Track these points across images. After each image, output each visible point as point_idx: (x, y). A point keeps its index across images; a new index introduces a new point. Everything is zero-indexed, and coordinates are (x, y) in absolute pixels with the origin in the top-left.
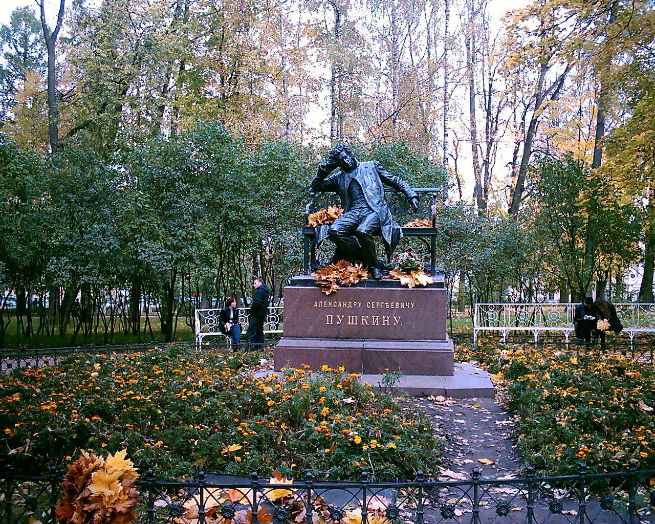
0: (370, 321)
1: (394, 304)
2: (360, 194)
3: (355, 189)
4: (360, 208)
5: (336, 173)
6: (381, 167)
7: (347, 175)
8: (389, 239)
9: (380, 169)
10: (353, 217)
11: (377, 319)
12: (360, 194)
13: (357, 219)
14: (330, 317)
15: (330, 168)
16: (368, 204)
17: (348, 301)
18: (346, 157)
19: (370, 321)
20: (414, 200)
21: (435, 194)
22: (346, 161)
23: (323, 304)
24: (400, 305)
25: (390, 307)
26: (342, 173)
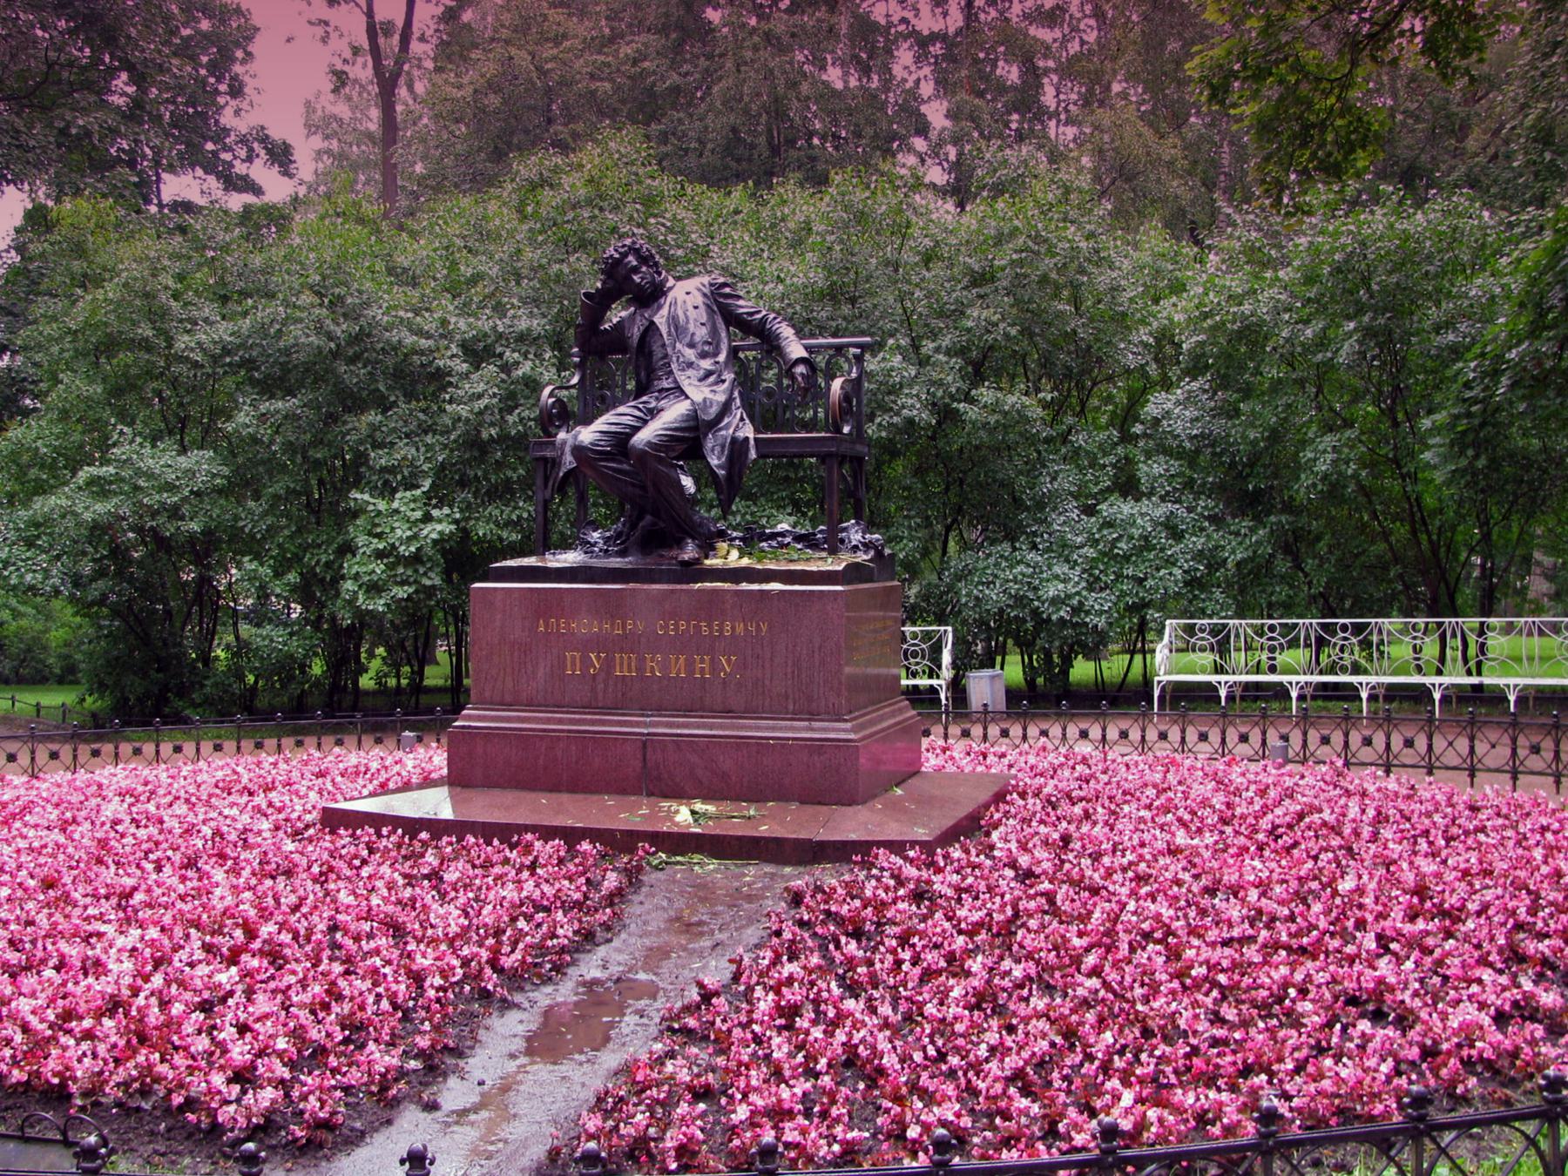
0: (665, 667)
1: (721, 626)
11: (682, 658)
14: (573, 658)
16: (675, 381)
18: (635, 270)
19: (665, 667)
22: (637, 278)
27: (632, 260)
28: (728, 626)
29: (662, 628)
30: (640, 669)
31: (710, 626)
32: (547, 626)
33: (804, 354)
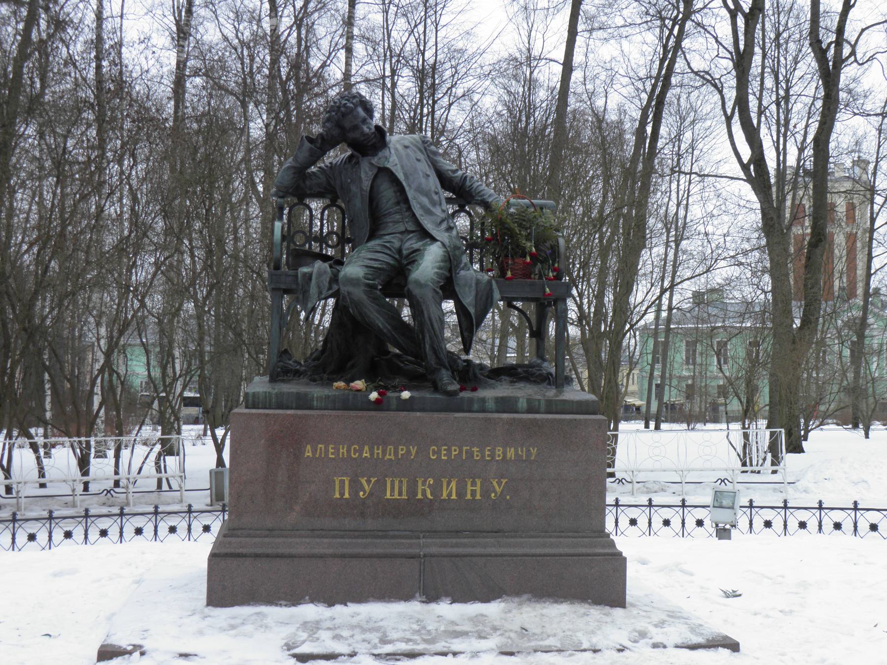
0: (436, 489)
2: (398, 203)
3: (387, 193)
4: (402, 233)
7: (366, 159)
8: (468, 300)
10: (389, 252)
13: (397, 256)
15: (322, 144)
17: (385, 444)
19: (436, 489)
23: (327, 451)
24: (505, 453)
25: (483, 456)
26: (351, 157)
28: (499, 451)
29: (434, 453)
30: (412, 491)
31: (482, 451)
32: (314, 451)
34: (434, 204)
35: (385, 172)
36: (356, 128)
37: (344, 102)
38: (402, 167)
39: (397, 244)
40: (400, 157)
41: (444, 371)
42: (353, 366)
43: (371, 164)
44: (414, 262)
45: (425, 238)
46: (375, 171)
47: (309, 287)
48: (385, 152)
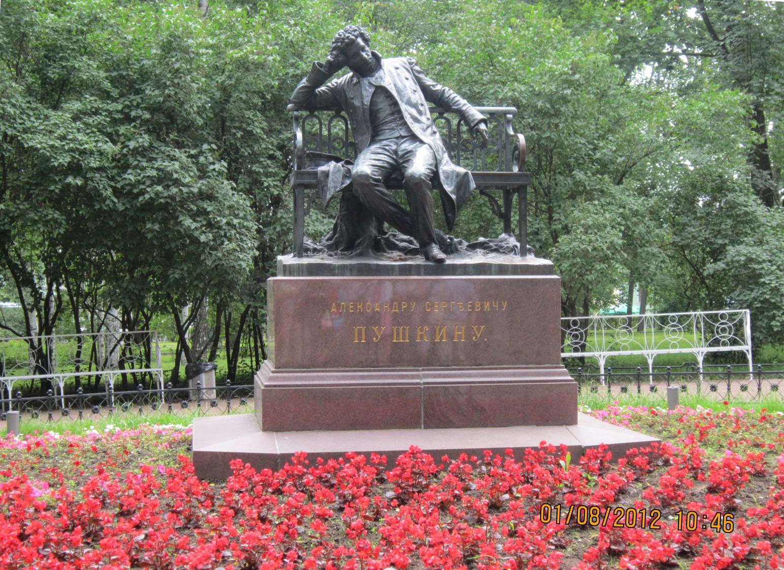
2: (392, 114)
4: (397, 138)
5: (342, 78)
6: (417, 68)
9: (419, 72)
12: (392, 114)
14: (360, 332)
16: (408, 129)
20: (482, 126)
21: (510, 116)
22: (364, 54)
24: (482, 306)
26: (352, 77)
27: (360, 40)
30: (412, 338)
33: (481, 116)
34: (420, 113)
35: (381, 90)
36: (357, 54)
37: (347, 35)
38: (395, 85)
39: (394, 147)
40: (392, 77)
41: (434, 245)
42: (359, 244)
43: (370, 83)
44: (408, 161)
45: (415, 142)
46: (372, 90)
47: (327, 183)
48: (381, 73)
